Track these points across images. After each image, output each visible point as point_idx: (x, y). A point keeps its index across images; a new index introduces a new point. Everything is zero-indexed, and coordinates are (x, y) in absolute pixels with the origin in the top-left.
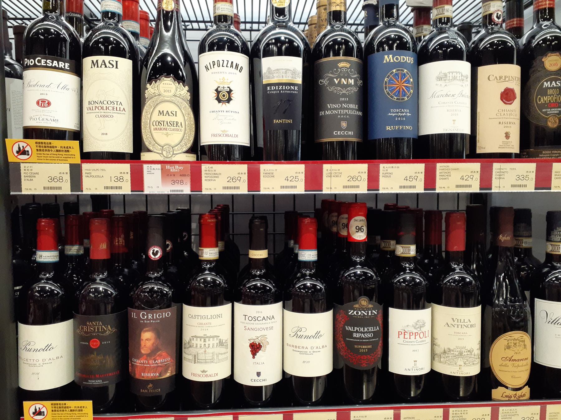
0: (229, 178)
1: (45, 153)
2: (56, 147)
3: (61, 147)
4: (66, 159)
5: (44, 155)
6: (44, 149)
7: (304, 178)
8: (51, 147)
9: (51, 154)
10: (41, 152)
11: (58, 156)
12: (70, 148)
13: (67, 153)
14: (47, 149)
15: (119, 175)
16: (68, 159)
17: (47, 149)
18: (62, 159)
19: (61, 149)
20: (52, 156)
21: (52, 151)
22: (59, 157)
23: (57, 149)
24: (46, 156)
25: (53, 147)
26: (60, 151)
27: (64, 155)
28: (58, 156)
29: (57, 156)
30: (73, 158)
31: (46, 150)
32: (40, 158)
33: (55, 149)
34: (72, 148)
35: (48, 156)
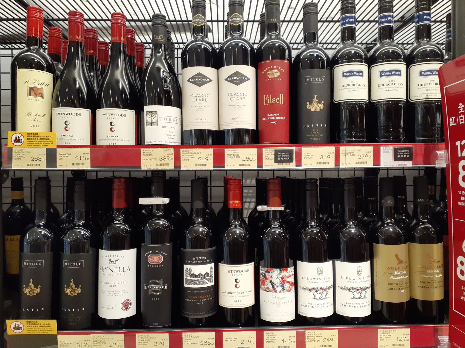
0: (244, 158)
1: (33, 140)
2: (41, 136)
3: (44, 136)
4: (47, 145)
5: (32, 142)
6: (33, 138)
7: (173, 158)
8: (37, 137)
9: (37, 142)
10: (31, 140)
11: (41, 143)
12: (50, 137)
13: (48, 141)
14: (35, 138)
15: (166, 156)
16: (48, 145)
17: (35, 138)
18: (44, 144)
19: (44, 138)
20: (37, 142)
21: (37, 139)
22: (42, 144)
23: (41, 138)
24: (33, 143)
25: (39, 136)
26: (43, 139)
27: (46, 142)
28: (41, 143)
29: (40, 143)
30: (51, 144)
31: (33, 139)
32: (29, 144)
33: (40, 138)
34: (51, 137)
35: (35, 143)
